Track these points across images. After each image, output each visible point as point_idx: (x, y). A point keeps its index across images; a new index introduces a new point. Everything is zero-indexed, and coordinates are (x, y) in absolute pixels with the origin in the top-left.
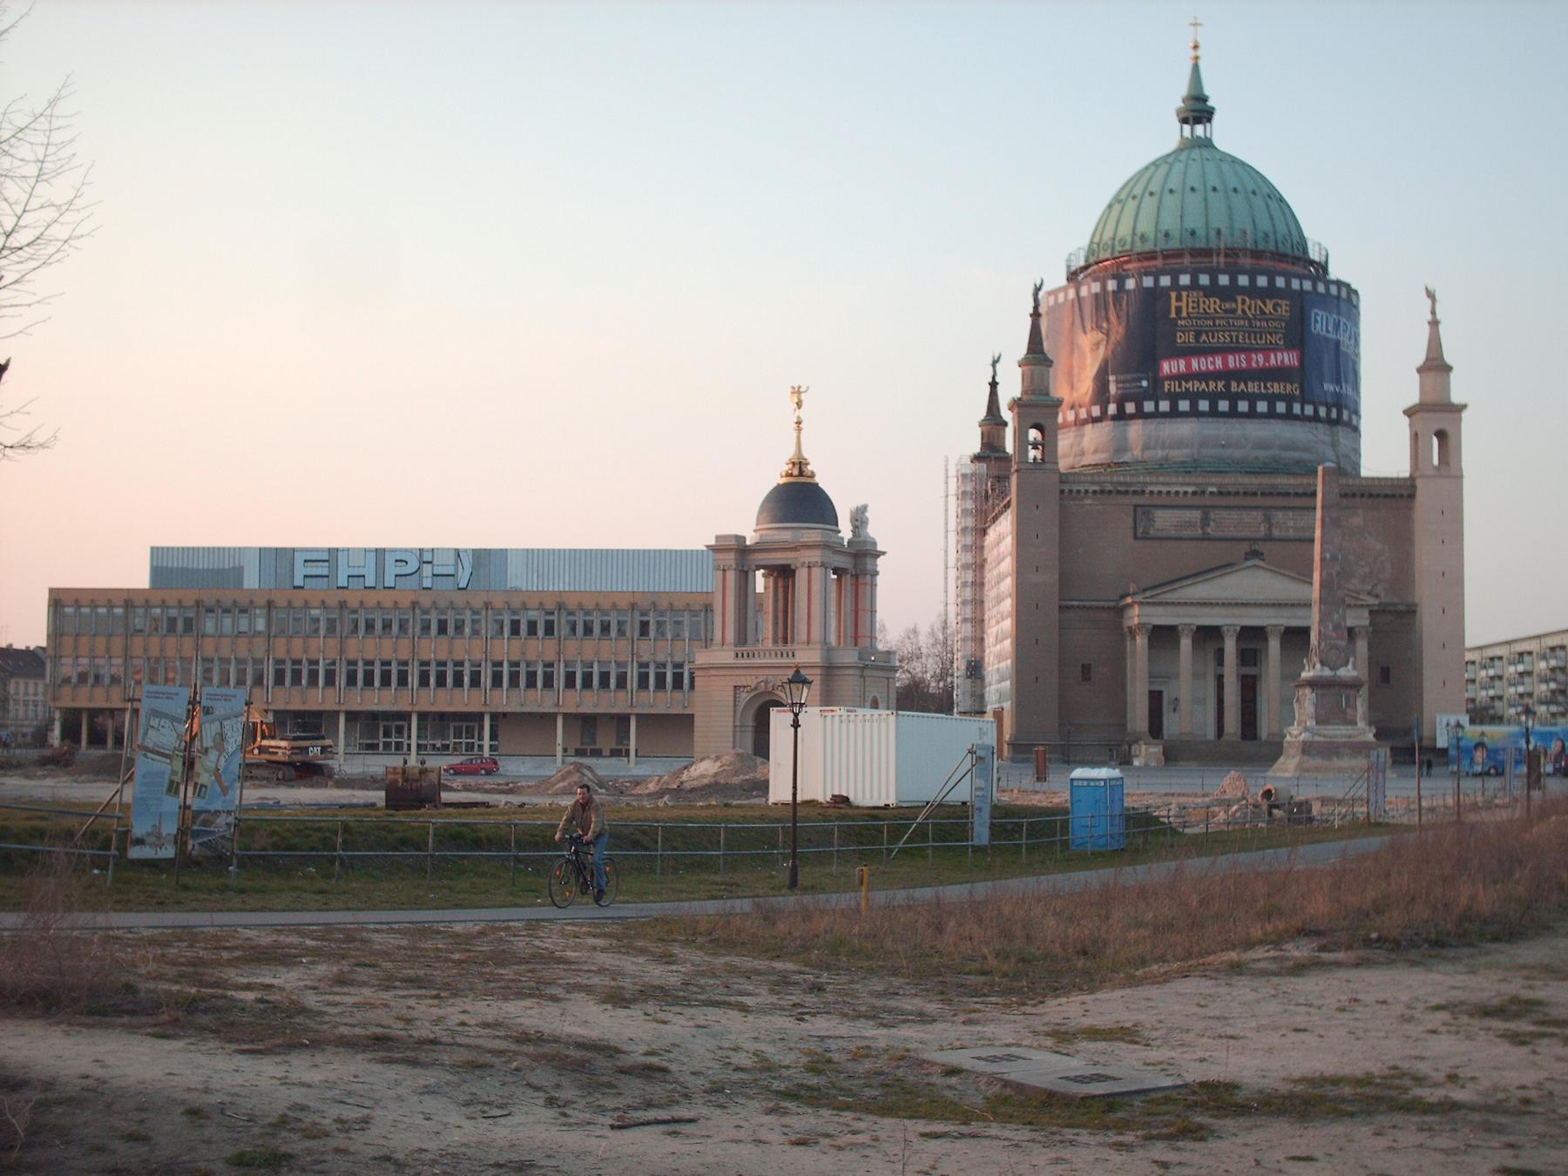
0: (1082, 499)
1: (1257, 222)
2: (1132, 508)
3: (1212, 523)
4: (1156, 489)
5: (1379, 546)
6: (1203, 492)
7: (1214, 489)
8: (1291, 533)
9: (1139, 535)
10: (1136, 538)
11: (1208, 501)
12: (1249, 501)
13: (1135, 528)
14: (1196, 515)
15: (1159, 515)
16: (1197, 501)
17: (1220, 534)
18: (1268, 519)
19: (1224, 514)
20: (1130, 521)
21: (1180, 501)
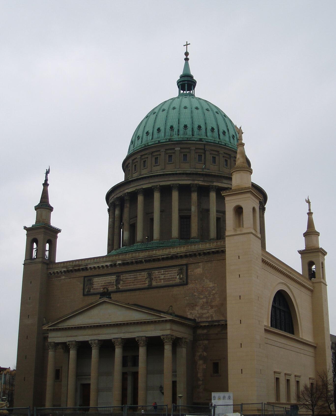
0: (60, 277)
1: (181, 120)
2: (83, 278)
3: (121, 282)
4: (92, 266)
5: (211, 285)
6: (115, 265)
7: (120, 262)
8: (162, 283)
9: (85, 293)
10: (84, 295)
11: (119, 269)
12: (140, 267)
13: (84, 289)
14: (114, 278)
15: (96, 280)
16: (114, 270)
17: (125, 288)
18: (150, 275)
19: (127, 276)
20: (82, 286)
21: (105, 271)
